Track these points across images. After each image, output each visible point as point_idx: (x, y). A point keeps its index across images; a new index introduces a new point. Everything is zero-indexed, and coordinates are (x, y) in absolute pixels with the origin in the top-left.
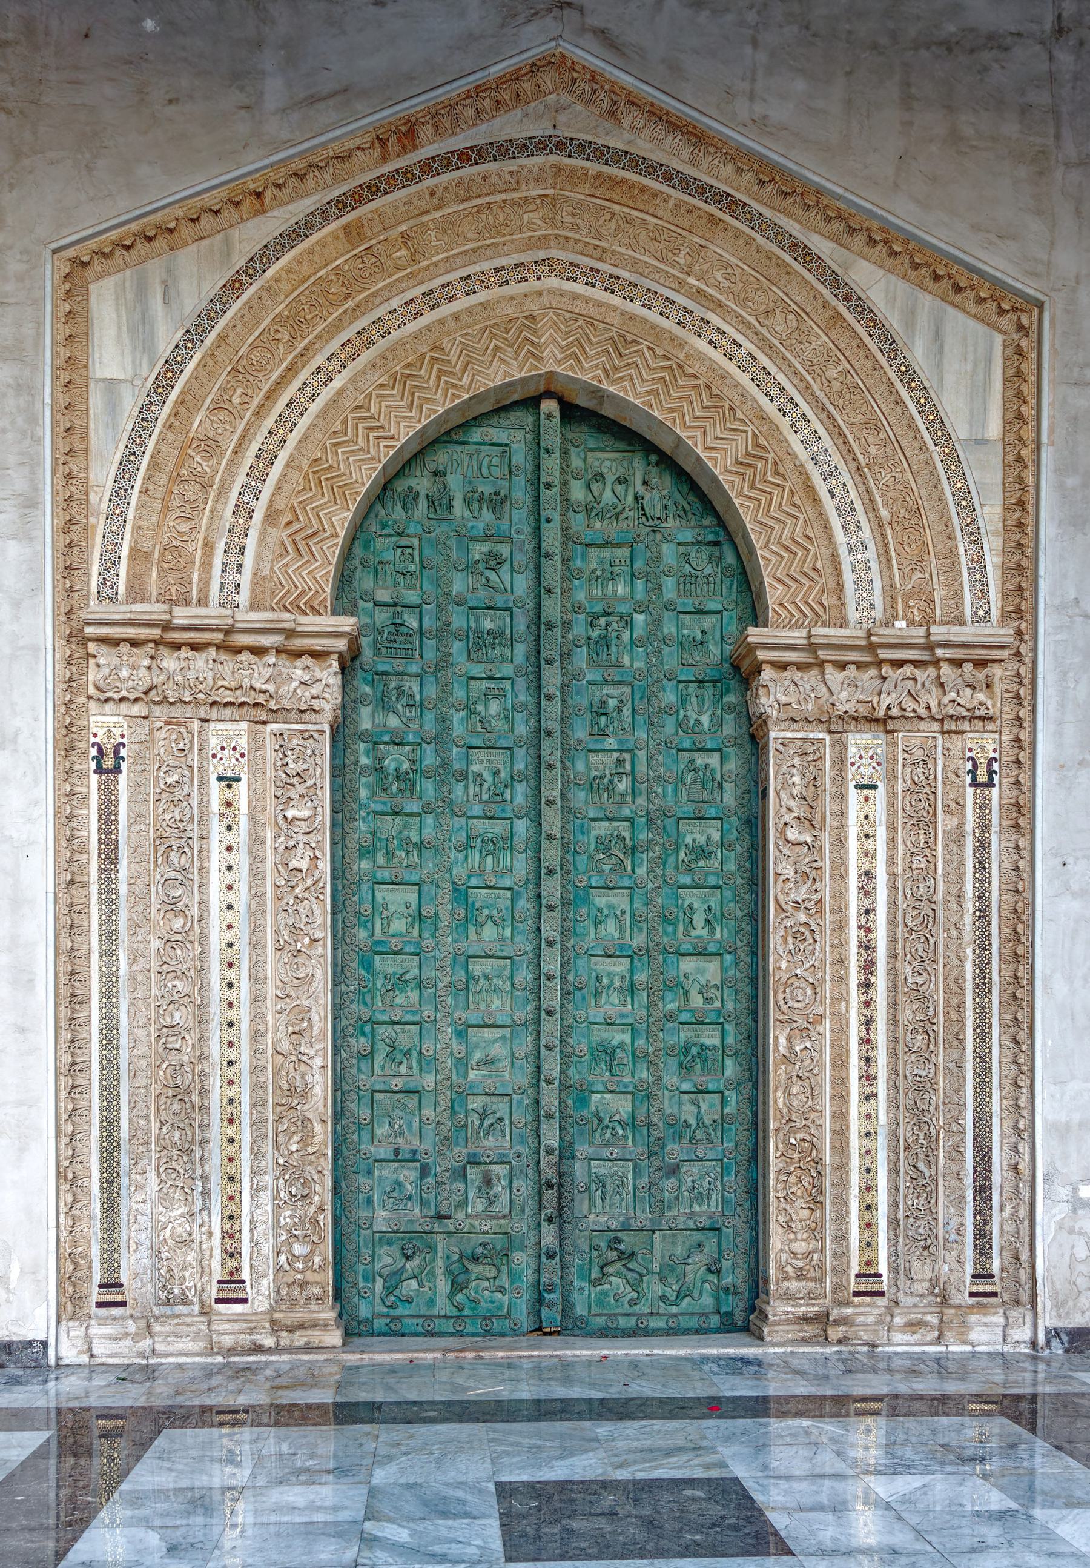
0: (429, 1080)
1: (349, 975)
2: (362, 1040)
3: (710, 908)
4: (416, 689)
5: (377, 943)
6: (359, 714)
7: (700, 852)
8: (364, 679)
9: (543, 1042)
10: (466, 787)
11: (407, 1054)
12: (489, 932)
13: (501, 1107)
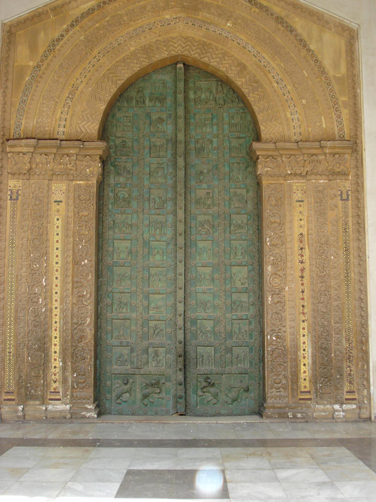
0: (134, 315)
1: (104, 274)
2: (108, 299)
3: (243, 248)
4: (131, 168)
5: (114, 262)
6: (109, 177)
7: (240, 227)
8: (111, 165)
9: (178, 300)
10: (149, 204)
11: (126, 304)
12: (158, 257)
13: (162, 325)
